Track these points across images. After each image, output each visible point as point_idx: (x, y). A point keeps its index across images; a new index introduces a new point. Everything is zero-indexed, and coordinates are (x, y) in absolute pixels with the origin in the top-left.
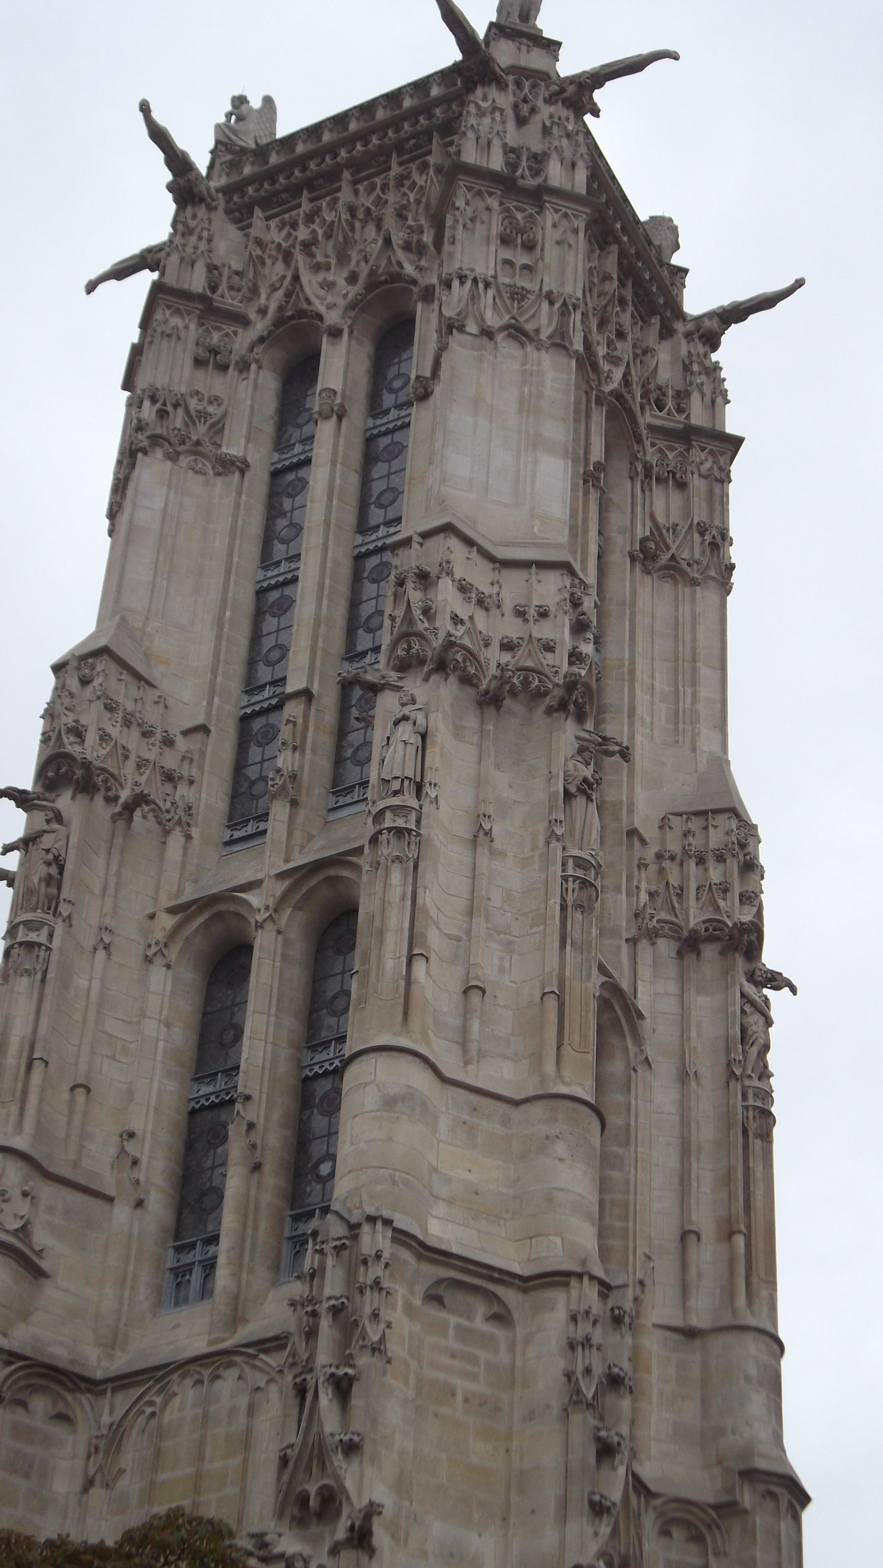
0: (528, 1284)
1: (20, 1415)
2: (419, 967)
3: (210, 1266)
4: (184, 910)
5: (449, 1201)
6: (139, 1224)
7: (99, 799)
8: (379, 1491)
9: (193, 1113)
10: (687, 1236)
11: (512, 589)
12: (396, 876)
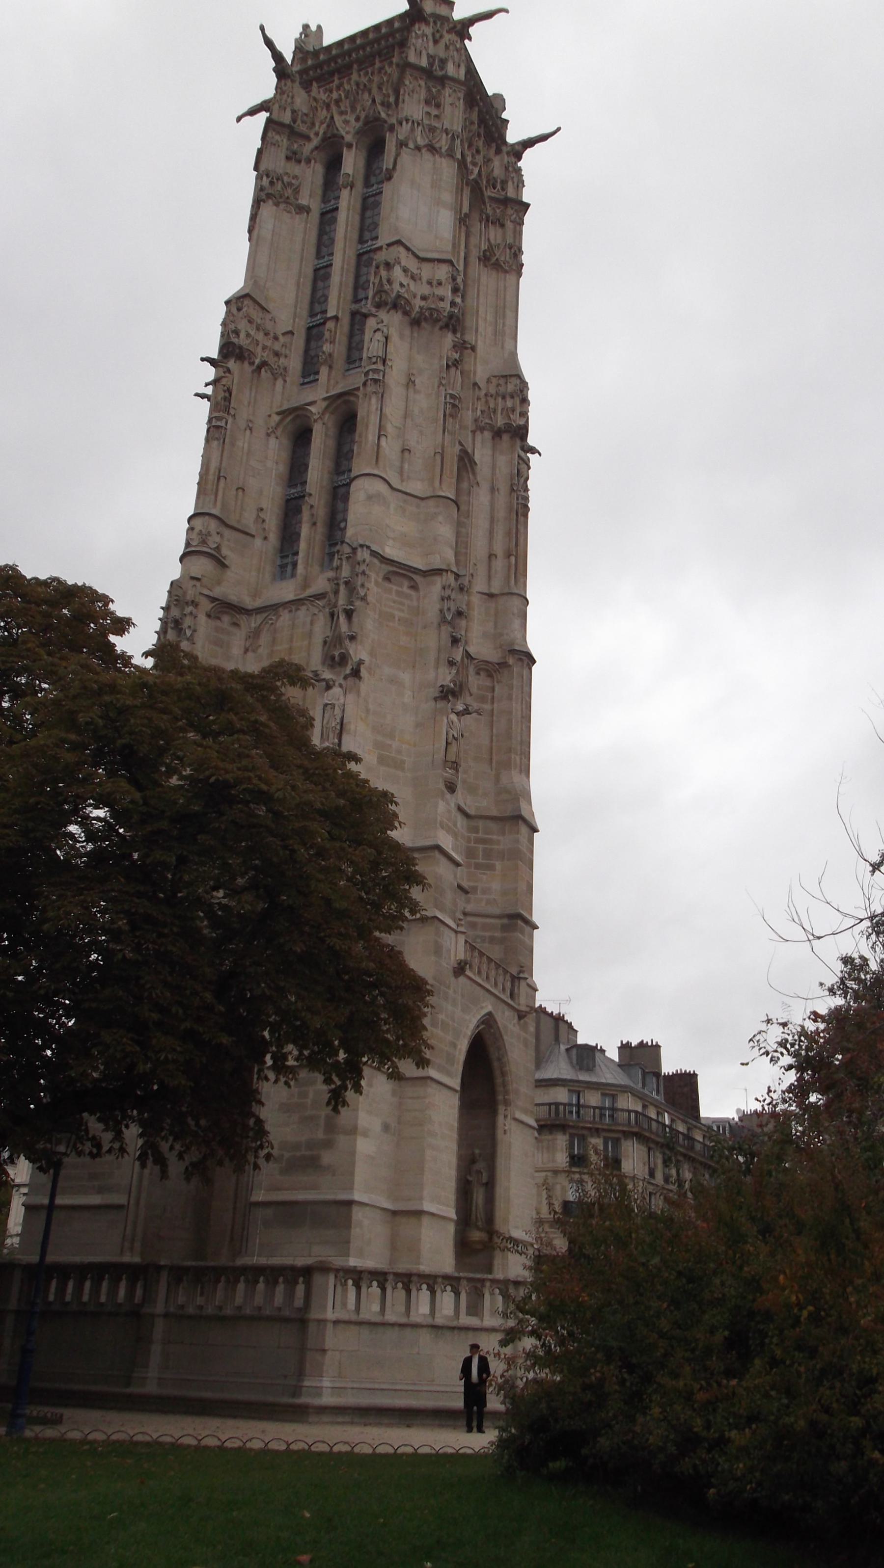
0: (426, 574)
1: (218, 623)
2: (383, 439)
3: (295, 565)
4: (282, 413)
5: (394, 539)
6: (265, 546)
7: (246, 364)
8: (364, 656)
9: (288, 501)
10: (491, 556)
11: (426, 271)
12: (374, 400)
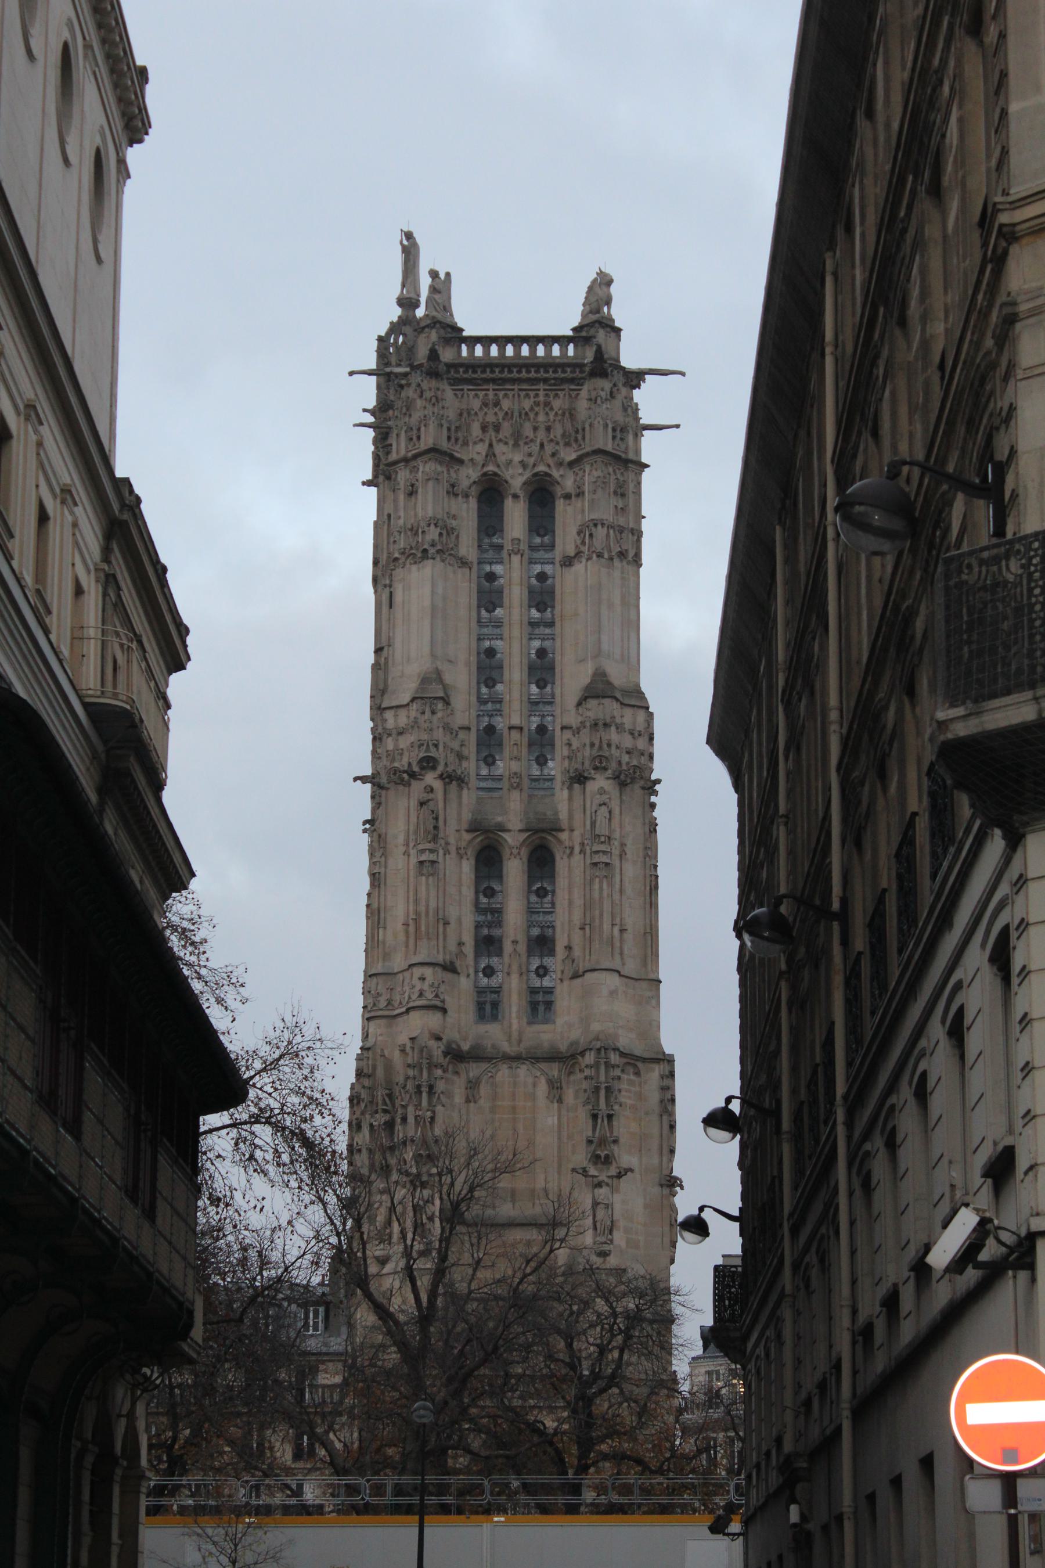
0: (644, 1060)
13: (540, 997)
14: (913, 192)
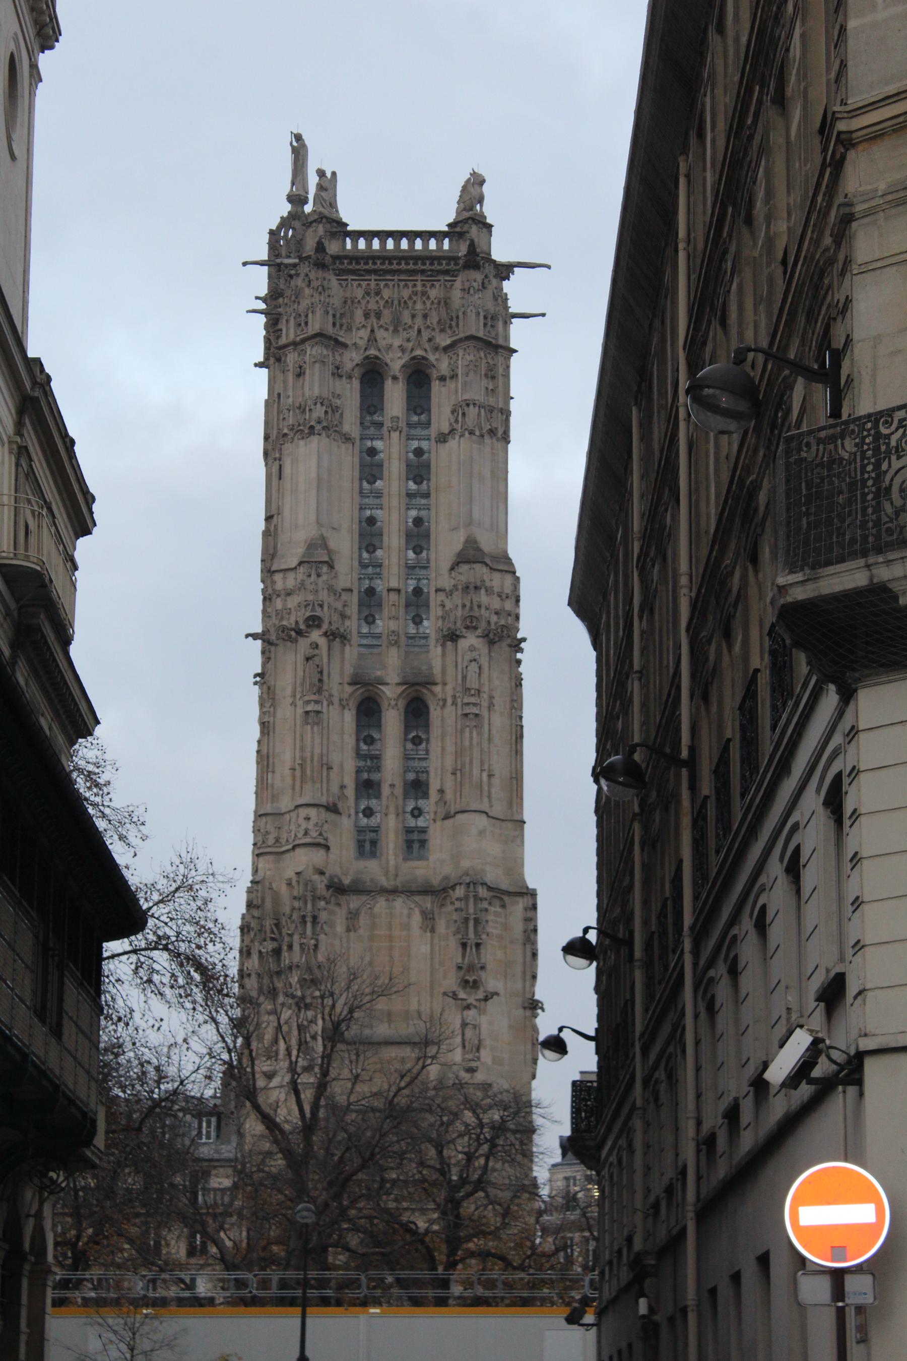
0: (509, 894)
13: (415, 836)
14: (760, 102)
